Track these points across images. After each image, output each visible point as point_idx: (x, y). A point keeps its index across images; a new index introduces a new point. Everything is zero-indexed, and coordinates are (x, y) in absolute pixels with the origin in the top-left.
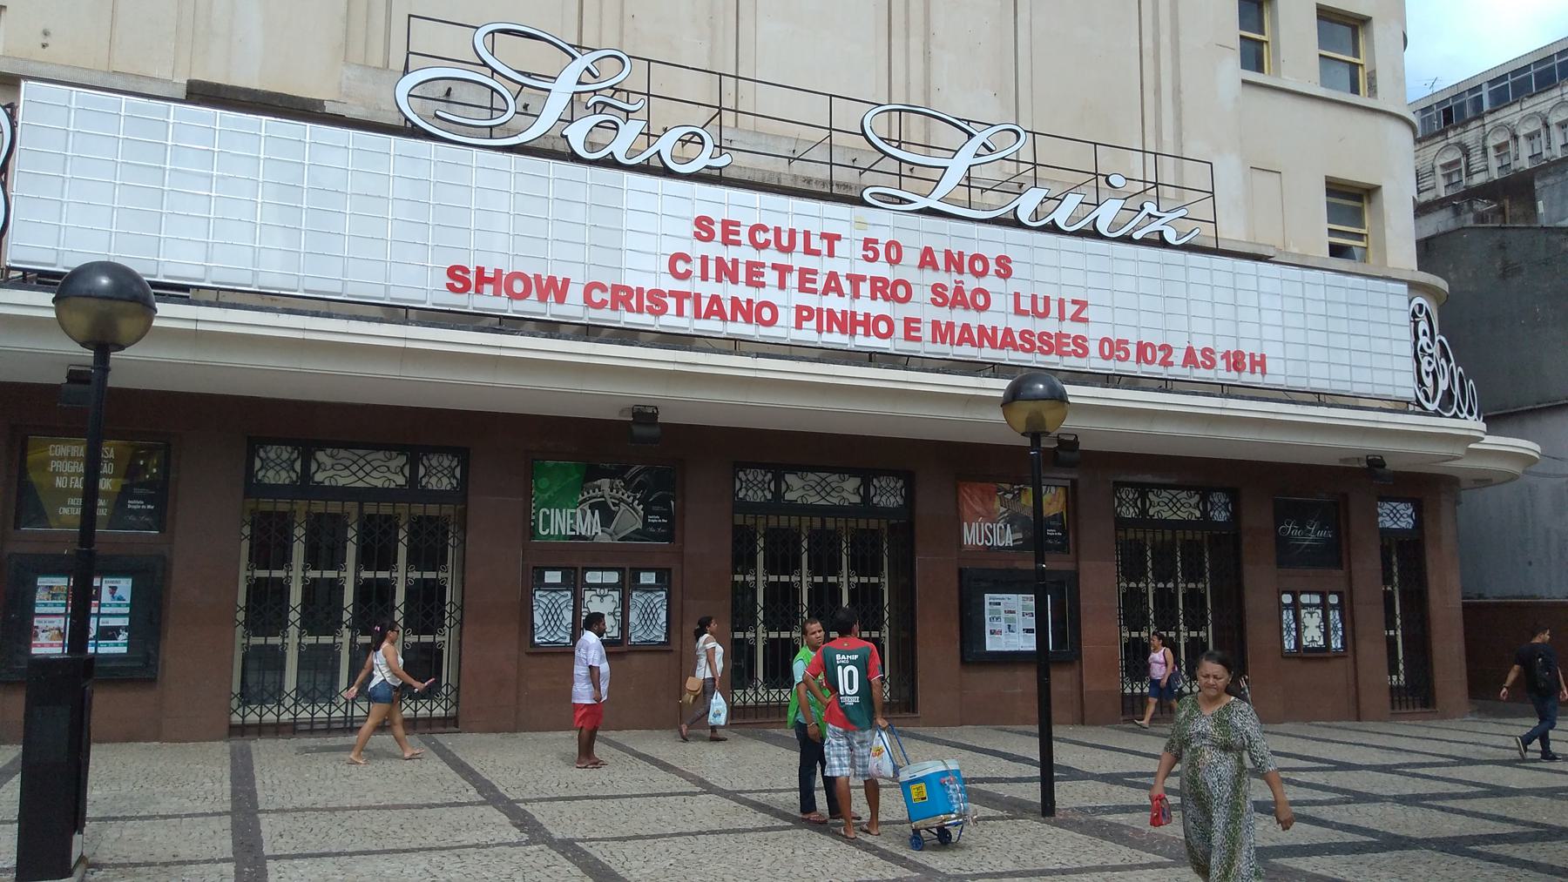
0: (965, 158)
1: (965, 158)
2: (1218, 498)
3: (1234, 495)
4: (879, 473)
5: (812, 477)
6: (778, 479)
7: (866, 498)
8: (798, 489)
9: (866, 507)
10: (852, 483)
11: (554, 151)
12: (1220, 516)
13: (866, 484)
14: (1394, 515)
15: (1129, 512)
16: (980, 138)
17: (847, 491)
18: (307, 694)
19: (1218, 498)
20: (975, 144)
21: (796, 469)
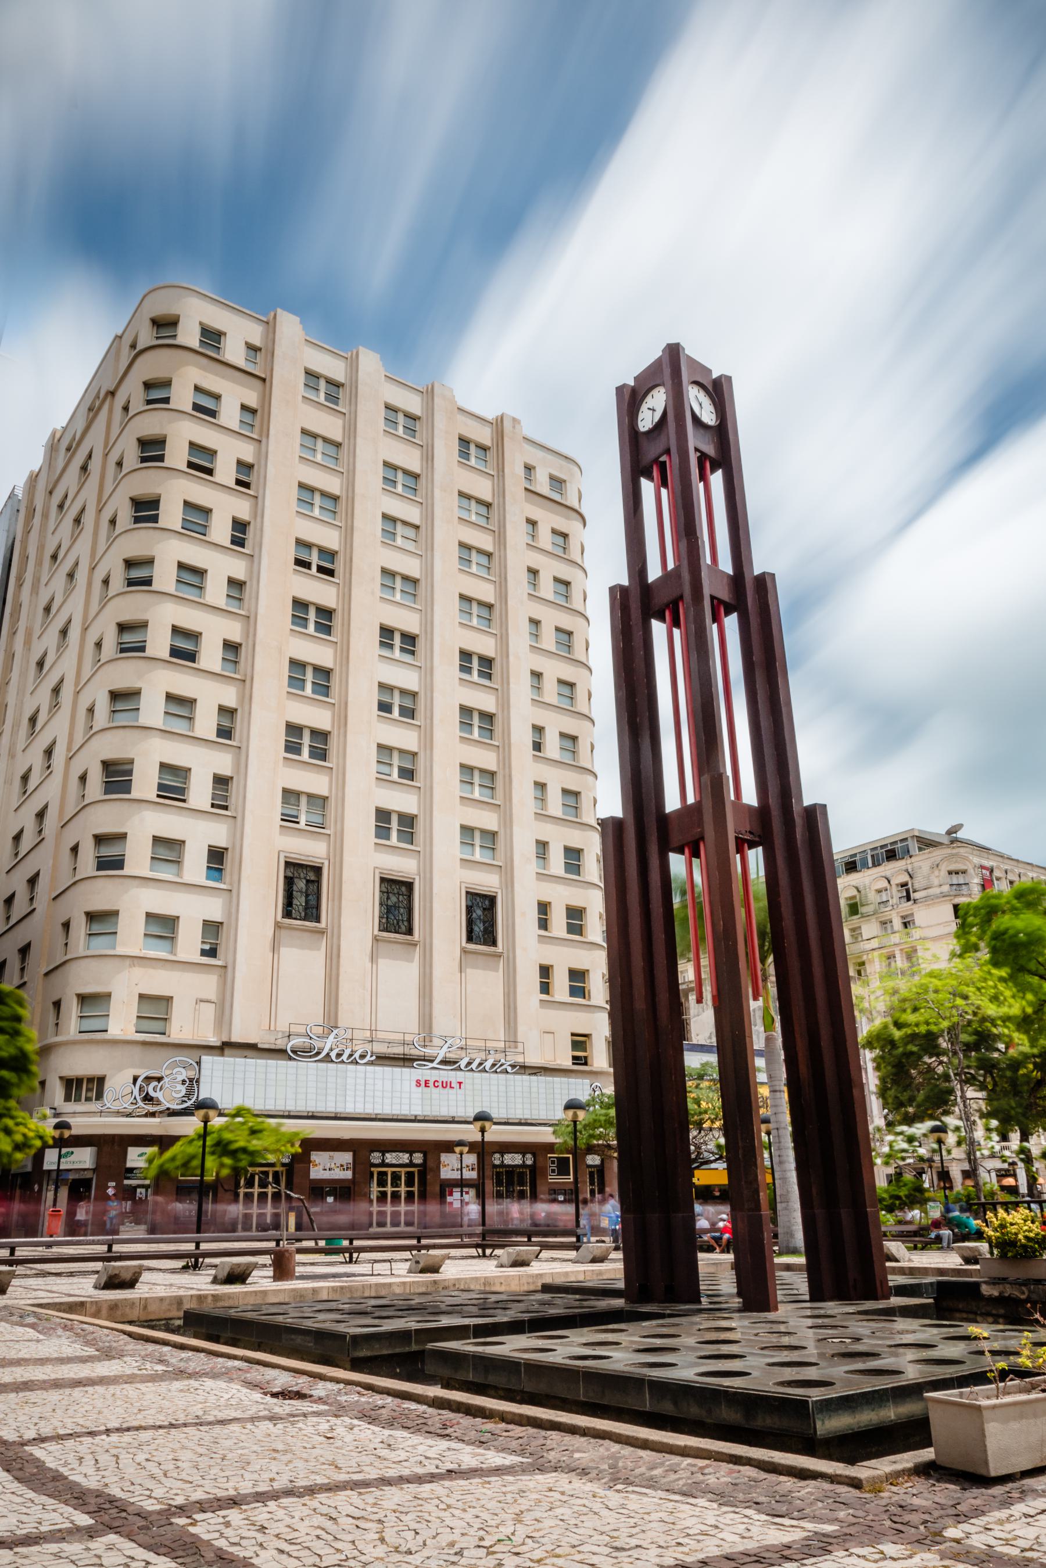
0: (445, 1049)
1: (445, 1049)
2: (529, 1156)
3: (534, 1155)
4: (415, 1152)
5: (394, 1154)
6: (383, 1155)
7: (411, 1161)
8: (390, 1158)
9: (411, 1164)
10: (407, 1155)
11: (328, 1059)
12: (529, 1162)
13: (411, 1156)
14: (593, 1160)
15: (497, 1162)
16: (449, 1042)
17: (405, 1158)
18: (245, 1229)
19: (529, 1156)
20: (447, 1045)
21: (388, 1152)
